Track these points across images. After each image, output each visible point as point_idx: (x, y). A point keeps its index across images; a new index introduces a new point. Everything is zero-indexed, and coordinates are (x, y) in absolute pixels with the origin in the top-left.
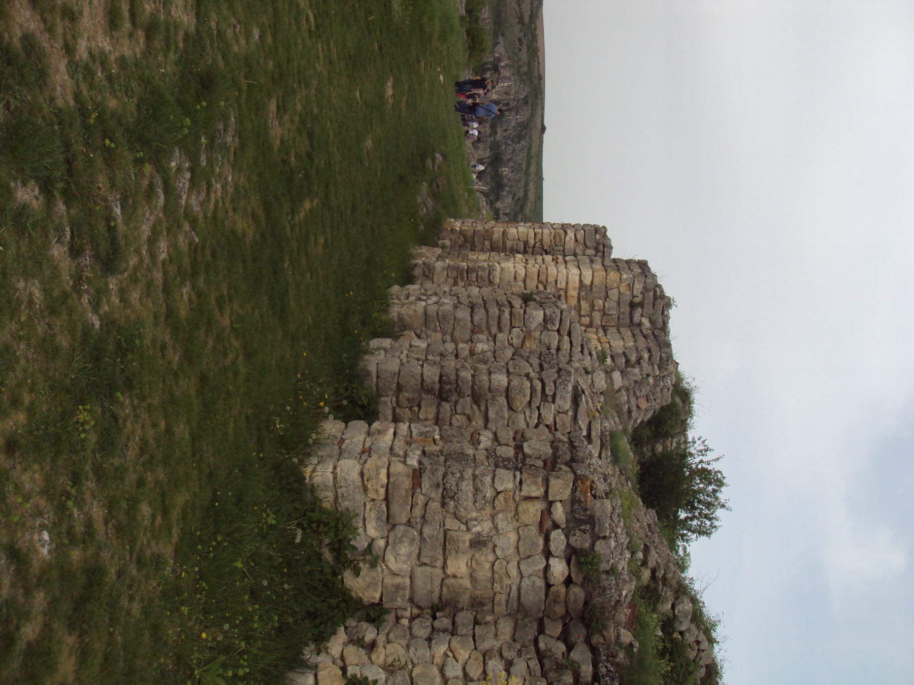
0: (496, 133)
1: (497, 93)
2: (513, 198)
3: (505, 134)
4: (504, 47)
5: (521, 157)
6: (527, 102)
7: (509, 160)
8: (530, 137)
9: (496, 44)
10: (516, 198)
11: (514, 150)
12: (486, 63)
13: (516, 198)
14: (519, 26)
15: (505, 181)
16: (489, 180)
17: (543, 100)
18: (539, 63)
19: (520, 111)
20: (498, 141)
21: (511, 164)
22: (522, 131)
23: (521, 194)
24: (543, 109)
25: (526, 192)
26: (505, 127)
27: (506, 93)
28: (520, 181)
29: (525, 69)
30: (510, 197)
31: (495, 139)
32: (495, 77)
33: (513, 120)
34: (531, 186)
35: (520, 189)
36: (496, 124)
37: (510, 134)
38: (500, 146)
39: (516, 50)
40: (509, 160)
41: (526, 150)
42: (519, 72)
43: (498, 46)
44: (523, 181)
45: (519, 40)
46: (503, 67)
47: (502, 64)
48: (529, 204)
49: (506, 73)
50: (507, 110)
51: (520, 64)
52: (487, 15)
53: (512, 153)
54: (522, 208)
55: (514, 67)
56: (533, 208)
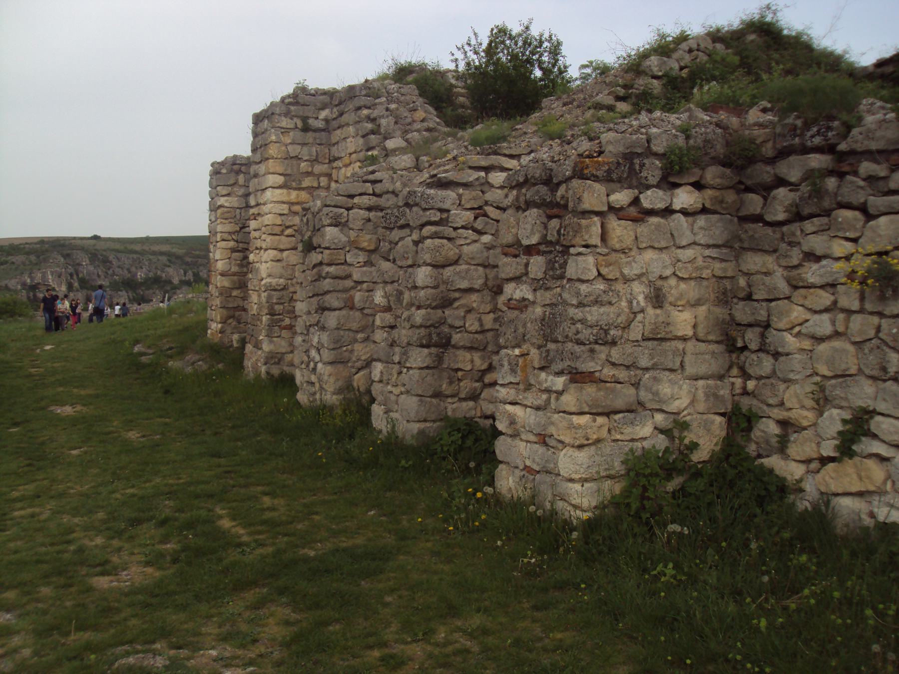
1: (60, 285)
2: (169, 266)
4: (11, 279)
7: (129, 272)
8: (105, 250)
10: (168, 263)
11: (119, 267)
12: (29, 298)
13: (168, 263)
15: (151, 275)
16: (151, 291)
17: (65, 239)
18: (27, 243)
21: (133, 269)
22: (99, 259)
23: (164, 259)
24: (74, 238)
25: (162, 253)
26: (95, 277)
27: (59, 277)
28: (150, 260)
29: (33, 258)
30: (167, 269)
31: (108, 287)
32: (43, 288)
33: (87, 268)
34: (156, 248)
35: (158, 260)
36: (92, 286)
38: (115, 280)
39: (14, 267)
40: (129, 272)
41: (119, 255)
42: (36, 264)
44: (151, 257)
47: (29, 281)
48: (174, 250)
49: (38, 277)
50: (78, 275)
51: (27, 263)
53: (122, 269)
54: (178, 257)
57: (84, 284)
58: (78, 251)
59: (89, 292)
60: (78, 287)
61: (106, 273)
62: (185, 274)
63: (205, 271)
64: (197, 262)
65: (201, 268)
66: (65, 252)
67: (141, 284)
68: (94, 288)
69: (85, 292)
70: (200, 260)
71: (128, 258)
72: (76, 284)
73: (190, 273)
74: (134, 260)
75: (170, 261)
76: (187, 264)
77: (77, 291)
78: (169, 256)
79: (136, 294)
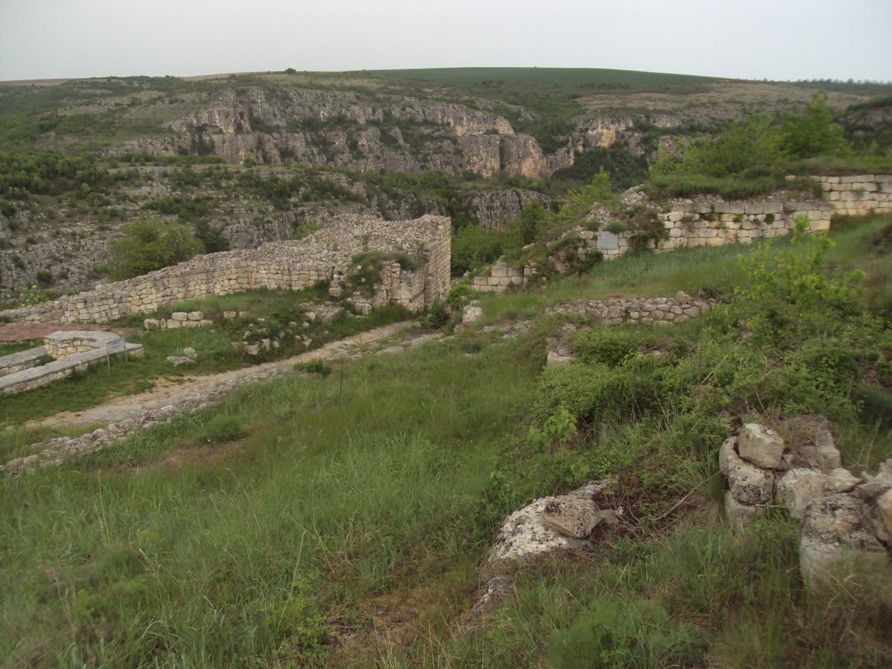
0: (278, 127)
1: (227, 127)
2: (355, 104)
3: (279, 116)
4: (175, 120)
5: (308, 96)
6: (243, 92)
7: (312, 110)
8: (286, 86)
9: (170, 130)
10: (355, 100)
11: (299, 105)
12: (194, 141)
13: (355, 100)
14: (159, 103)
15: (334, 114)
16: (334, 133)
17: (251, 74)
18: (216, 79)
19: (253, 98)
20: (288, 123)
21: (316, 107)
22: (277, 96)
23: (351, 95)
24: (269, 73)
25: (351, 89)
26: (271, 116)
27: (227, 117)
28: (335, 96)
29: (204, 95)
30: (353, 107)
31: (285, 128)
32: (210, 130)
33: (262, 107)
34: (347, 83)
35: (345, 96)
36: (267, 127)
37: (279, 109)
38: (295, 120)
39: (182, 105)
40: (312, 110)
41: (301, 91)
42: (205, 102)
43: (173, 127)
44: (337, 93)
45: (171, 102)
46: (198, 122)
47: (195, 122)
49: (205, 118)
50: (251, 114)
51: (197, 100)
52: (135, 143)
53: (303, 106)
54: (369, 93)
55: (198, 108)
56: (377, 80)
57: (256, 124)
58: (255, 88)
59: (262, 135)
60: (249, 129)
61: (284, 111)
62: (374, 112)
63: (398, 109)
64: (390, 98)
66: (240, 88)
67: (325, 124)
68: (270, 131)
69: (257, 133)
70: (393, 97)
71: (311, 94)
72: (246, 125)
74: (317, 97)
75: (357, 97)
76: (378, 100)
77: (248, 132)
79: (318, 136)
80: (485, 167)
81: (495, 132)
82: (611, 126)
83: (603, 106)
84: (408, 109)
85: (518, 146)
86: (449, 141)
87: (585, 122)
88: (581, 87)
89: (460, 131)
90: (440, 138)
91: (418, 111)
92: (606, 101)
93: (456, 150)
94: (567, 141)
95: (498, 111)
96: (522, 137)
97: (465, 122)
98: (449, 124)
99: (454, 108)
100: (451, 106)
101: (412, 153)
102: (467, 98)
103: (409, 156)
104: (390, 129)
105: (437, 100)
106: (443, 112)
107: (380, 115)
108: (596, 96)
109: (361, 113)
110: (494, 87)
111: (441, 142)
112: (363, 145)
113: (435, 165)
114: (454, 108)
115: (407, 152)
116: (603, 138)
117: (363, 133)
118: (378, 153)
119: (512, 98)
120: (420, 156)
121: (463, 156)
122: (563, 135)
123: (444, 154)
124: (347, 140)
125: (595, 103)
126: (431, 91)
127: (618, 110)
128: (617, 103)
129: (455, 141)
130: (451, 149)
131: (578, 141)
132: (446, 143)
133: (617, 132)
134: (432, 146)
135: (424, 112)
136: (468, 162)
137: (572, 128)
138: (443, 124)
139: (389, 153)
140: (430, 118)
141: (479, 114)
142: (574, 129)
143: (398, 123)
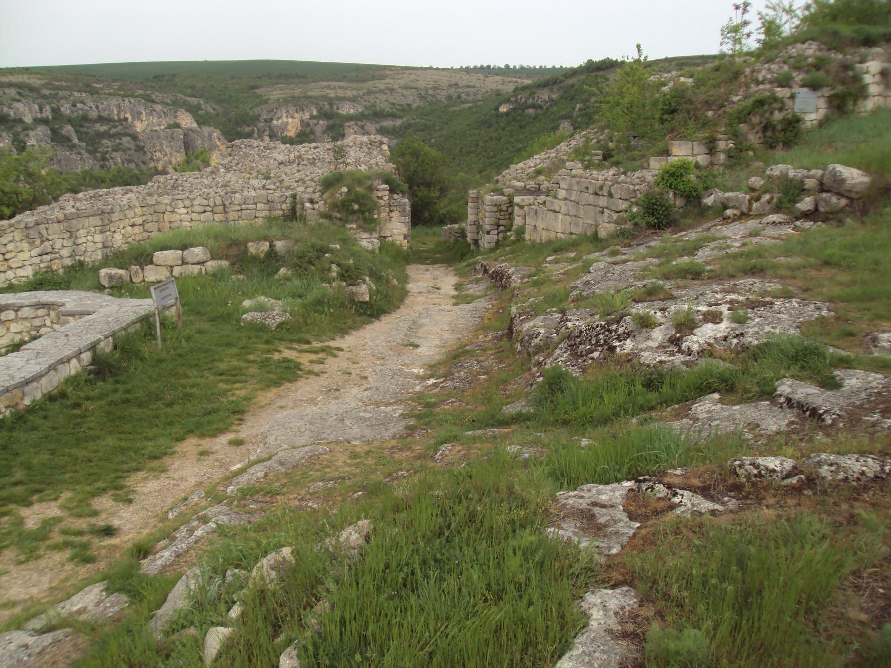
2: (19, 101)
10: (18, 97)
13: (18, 97)
23: (12, 92)
25: (11, 85)
30: (16, 105)
35: (5, 93)
48: (31, 81)
54: (32, 89)
56: (39, 76)
62: (41, 110)
63: (68, 106)
64: (57, 94)
65: (63, 102)
70: (60, 93)
73: (48, 108)
75: (20, 94)
76: (44, 97)
78: (20, 87)
80: (170, 162)
81: (178, 126)
82: (296, 115)
83: (284, 96)
84: (79, 105)
85: (203, 140)
86: (128, 138)
87: (269, 112)
88: (259, 78)
89: (139, 127)
90: (119, 135)
91: (90, 106)
92: (287, 91)
93: (137, 146)
94: (253, 132)
95: (177, 105)
96: (206, 130)
97: (143, 117)
98: (126, 119)
99: (130, 102)
100: (127, 100)
101: (89, 152)
102: (141, 92)
103: (86, 155)
104: (61, 127)
105: (110, 94)
106: (119, 107)
107: (48, 113)
108: (276, 86)
109: (26, 111)
110: (167, 81)
111: (120, 139)
112: (33, 146)
113: (115, 164)
114: (130, 102)
115: (83, 152)
116: (289, 128)
117: (31, 133)
118: (51, 154)
119: (189, 91)
120: (98, 155)
121: (145, 153)
122: (249, 126)
123: (124, 151)
124: (14, 141)
125: (276, 93)
126: (101, 85)
127: (299, 98)
128: (297, 92)
129: (134, 137)
130: (132, 146)
131: (264, 132)
132: (126, 140)
133: (302, 121)
134: (110, 144)
135: (97, 107)
136: (152, 159)
137: (256, 118)
138: (120, 120)
139: (63, 153)
140: (105, 114)
141: (159, 107)
142: (258, 119)
143: (70, 121)
